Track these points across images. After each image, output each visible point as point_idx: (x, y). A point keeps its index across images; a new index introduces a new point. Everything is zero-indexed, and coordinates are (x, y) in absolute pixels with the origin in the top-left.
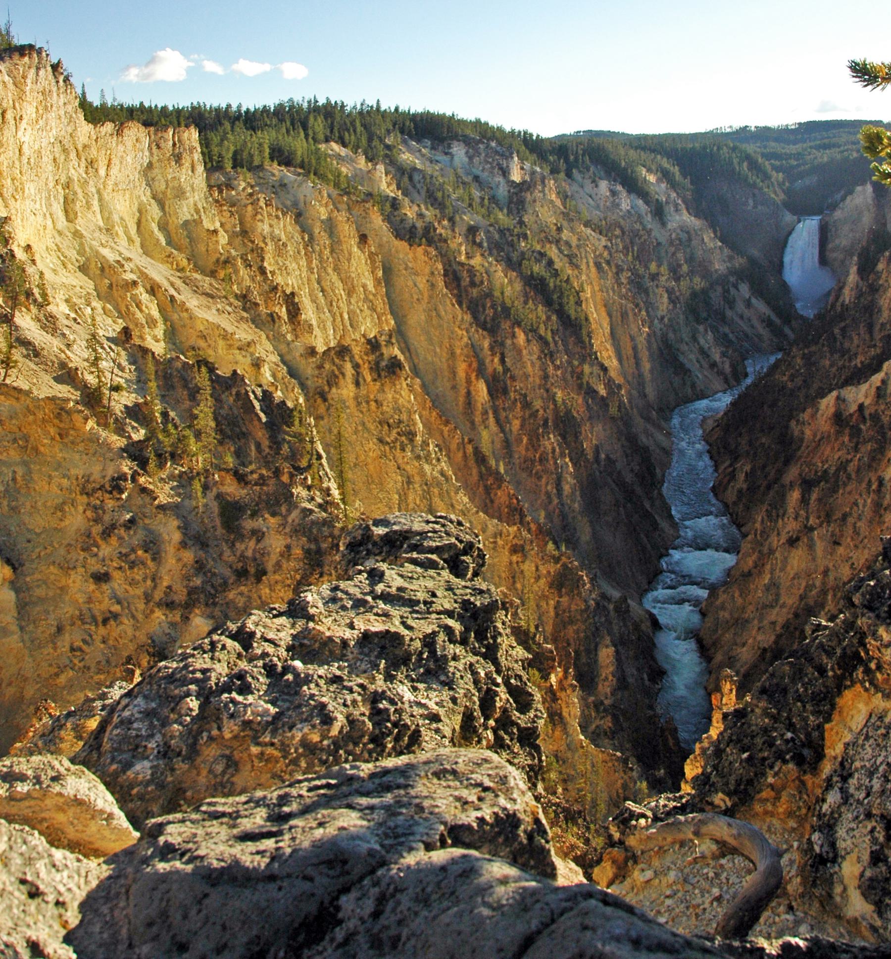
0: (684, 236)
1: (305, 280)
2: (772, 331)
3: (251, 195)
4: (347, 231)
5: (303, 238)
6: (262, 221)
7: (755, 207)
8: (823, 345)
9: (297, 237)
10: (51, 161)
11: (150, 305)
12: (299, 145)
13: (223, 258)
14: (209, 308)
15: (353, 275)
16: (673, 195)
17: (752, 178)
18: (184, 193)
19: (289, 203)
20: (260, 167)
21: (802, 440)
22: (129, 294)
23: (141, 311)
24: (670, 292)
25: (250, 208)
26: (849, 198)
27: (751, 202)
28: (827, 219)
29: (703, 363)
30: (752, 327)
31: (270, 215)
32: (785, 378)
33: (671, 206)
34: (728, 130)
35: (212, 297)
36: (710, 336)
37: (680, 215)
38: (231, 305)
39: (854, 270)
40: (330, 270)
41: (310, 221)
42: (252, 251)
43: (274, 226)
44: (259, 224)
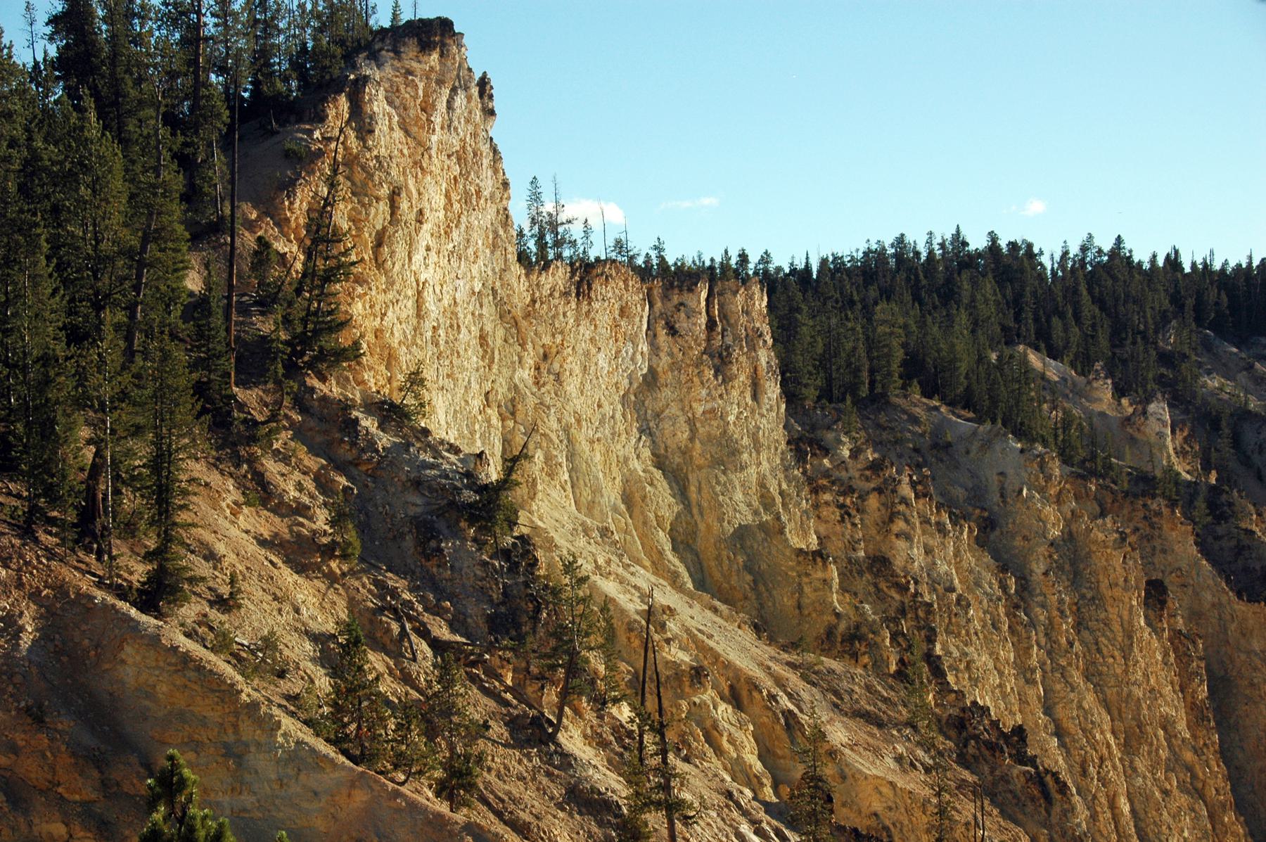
1: (1013, 699)
3: (876, 467)
4: (1118, 570)
5: (1004, 587)
6: (908, 538)
9: (989, 581)
10: (474, 342)
11: (739, 735)
12: (958, 344)
13: (842, 626)
14: (877, 752)
15: (1138, 692)
18: (735, 452)
19: (959, 493)
20: (877, 400)
22: (684, 705)
23: (719, 751)
25: (873, 502)
31: (925, 521)
35: (880, 725)
38: (928, 746)
40: (1077, 677)
41: (1018, 542)
42: (902, 612)
43: (936, 553)
44: (901, 544)
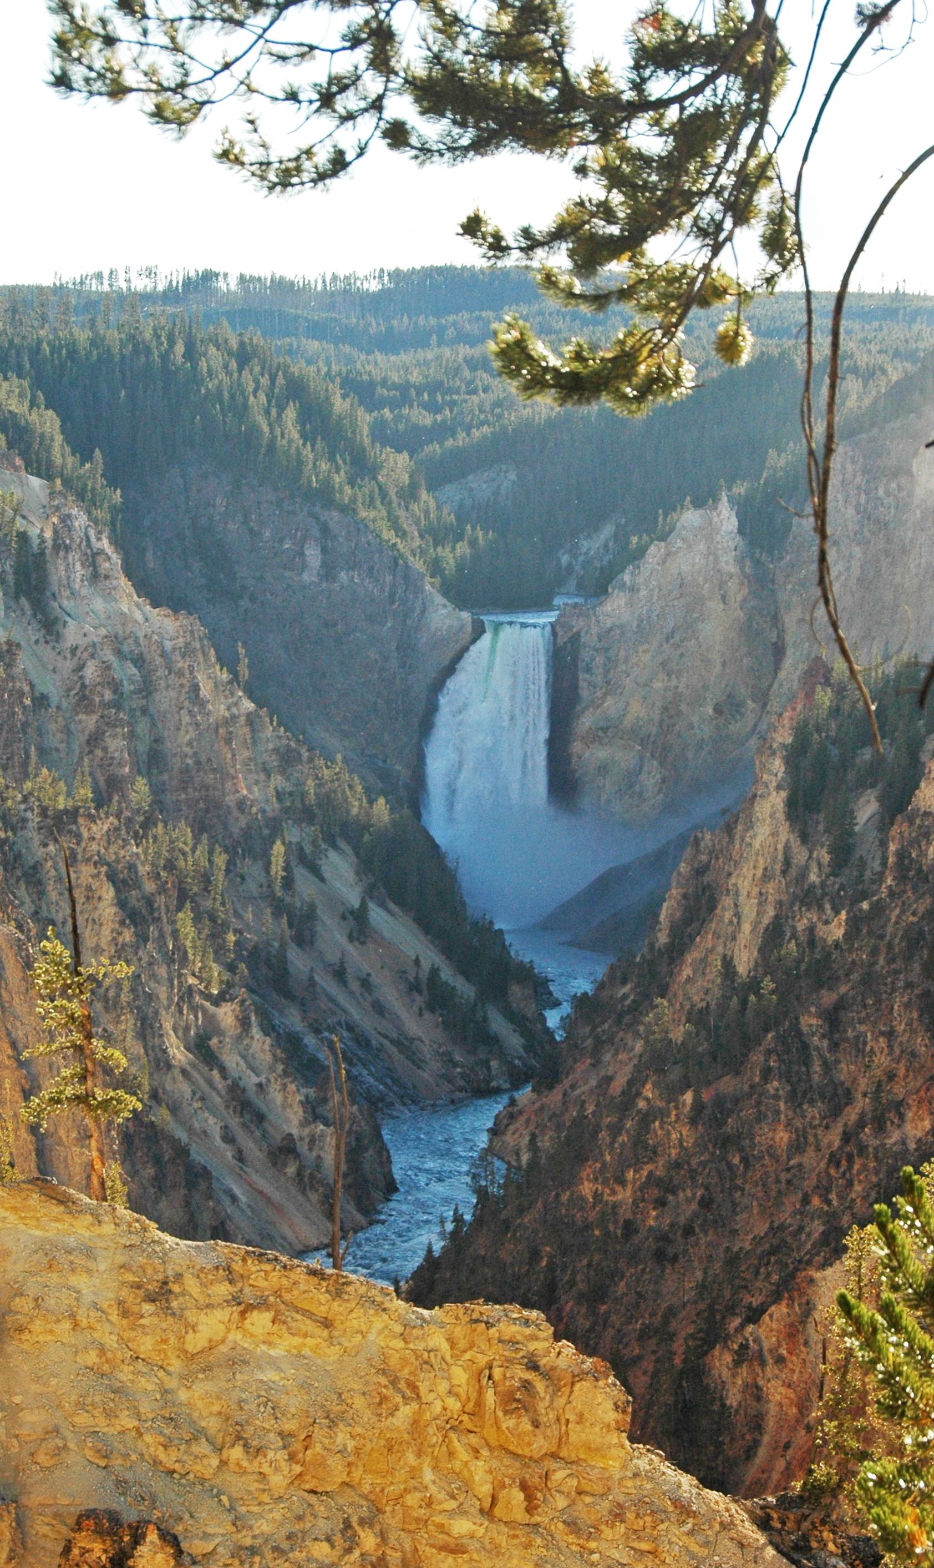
0: (128, 673)
2: (446, 1025)
7: (328, 572)
8: (767, 1074)
16: (80, 520)
17: (318, 467)
21: (757, 1424)
24: (123, 881)
26: (655, 552)
27: (313, 555)
28: (578, 624)
29: (248, 1144)
30: (379, 1009)
32: (625, 1195)
33: (75, 557)
34: (140, 284)
36: (260, 1044)
37: (109, 596)
39: (772, 804)
